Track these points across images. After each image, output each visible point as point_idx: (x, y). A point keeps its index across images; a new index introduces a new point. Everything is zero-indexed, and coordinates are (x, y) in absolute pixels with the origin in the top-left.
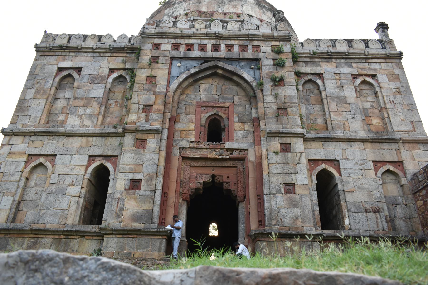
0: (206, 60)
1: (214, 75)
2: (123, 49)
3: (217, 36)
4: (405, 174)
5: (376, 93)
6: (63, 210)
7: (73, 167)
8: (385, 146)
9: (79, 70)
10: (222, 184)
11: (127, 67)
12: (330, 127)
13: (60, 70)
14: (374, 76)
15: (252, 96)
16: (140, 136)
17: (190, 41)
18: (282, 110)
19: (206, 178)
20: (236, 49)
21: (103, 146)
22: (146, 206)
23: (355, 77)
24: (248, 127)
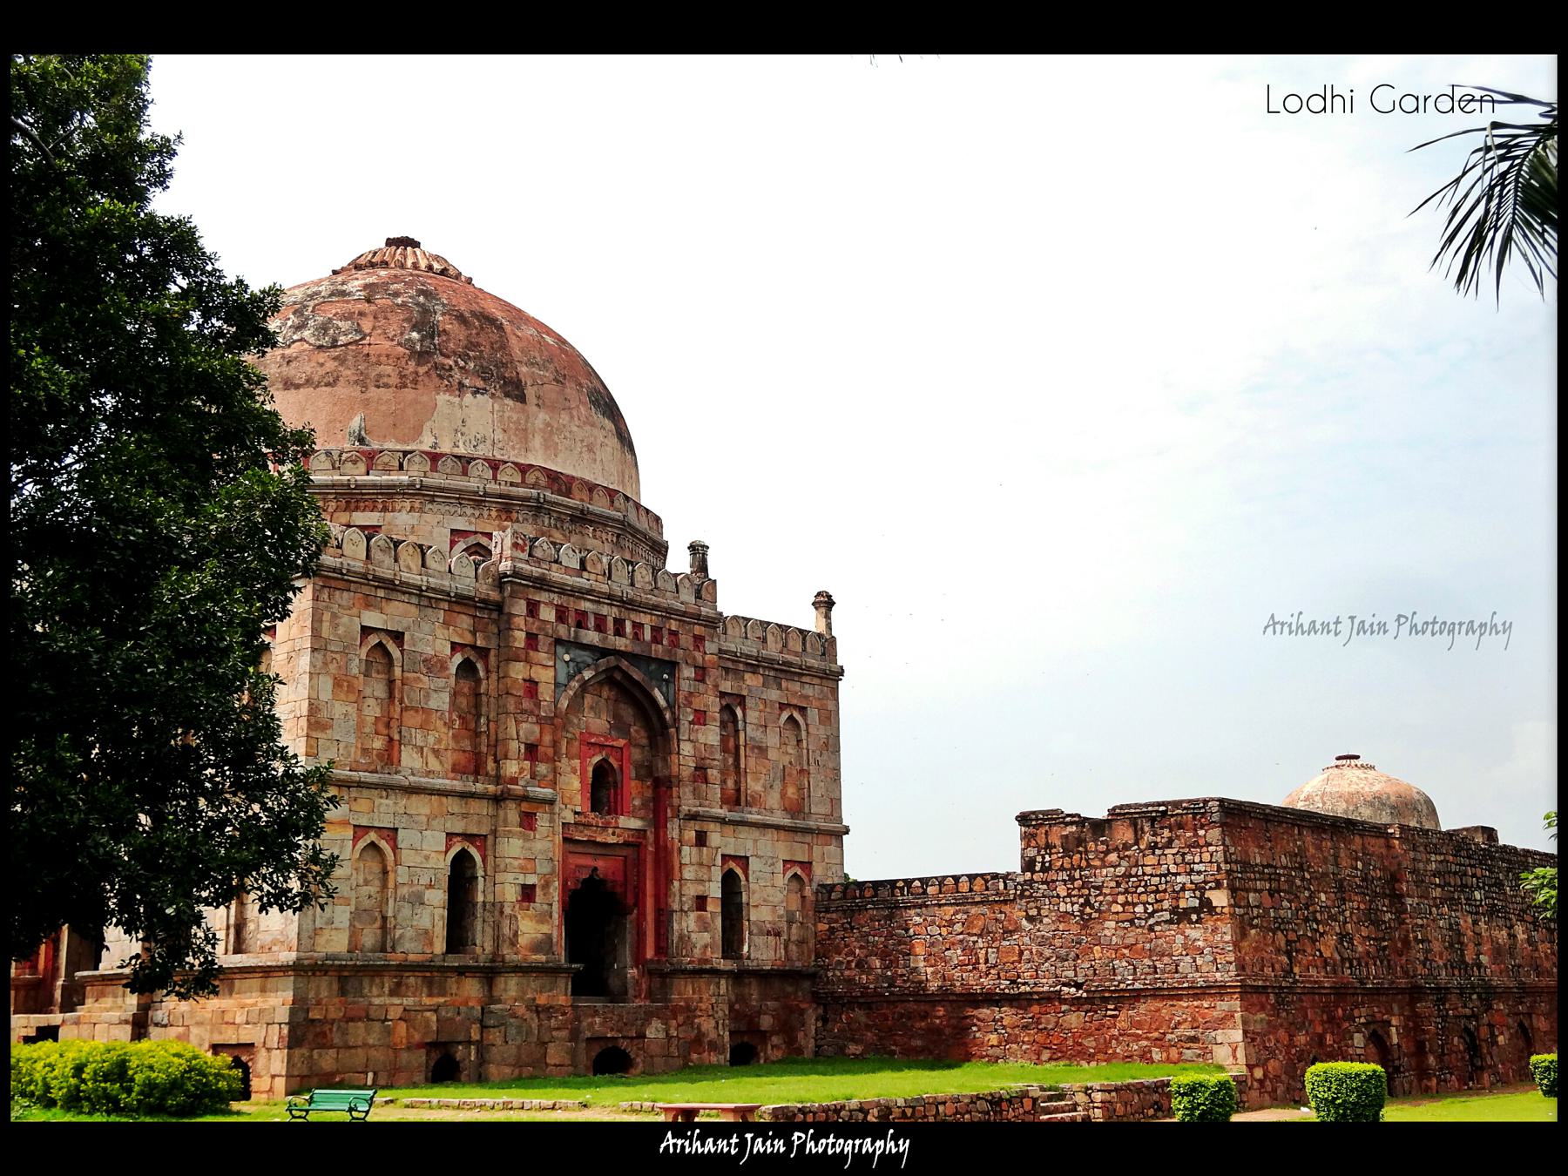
0: (603, 652)
2: (471, 599)
5: (799, 741)
6: (426, 932)
7: (426, 853)
9: (398, 637)
11: (479, 643)
13: (366, 631)
16: (525, 807)
18: (701, 773)
19: (585, 876)
21: (465, 816)
22: (545, 929)
23: (782, 706)
24: (649, 794)
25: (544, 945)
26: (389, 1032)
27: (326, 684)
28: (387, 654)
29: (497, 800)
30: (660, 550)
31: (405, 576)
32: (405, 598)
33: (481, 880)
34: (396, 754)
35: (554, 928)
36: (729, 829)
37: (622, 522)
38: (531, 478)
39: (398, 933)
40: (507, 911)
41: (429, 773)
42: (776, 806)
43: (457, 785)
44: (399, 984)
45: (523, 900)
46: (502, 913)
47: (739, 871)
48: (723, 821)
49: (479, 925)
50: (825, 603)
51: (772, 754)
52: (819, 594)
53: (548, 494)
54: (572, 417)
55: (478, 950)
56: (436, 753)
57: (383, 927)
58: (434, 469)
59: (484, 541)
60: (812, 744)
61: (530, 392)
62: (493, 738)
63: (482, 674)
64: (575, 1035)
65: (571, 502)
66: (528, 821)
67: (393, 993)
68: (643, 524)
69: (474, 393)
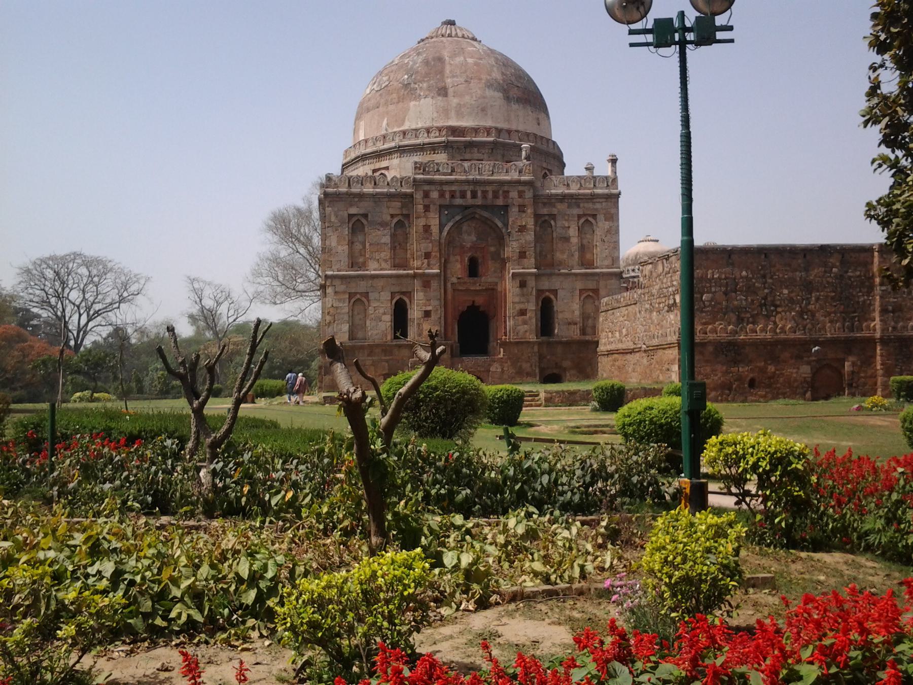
0: (467, 208)
1: (474, 218)
10: (478, 307)
19: (469, 304)
23: (579, 217)
47: (552, 297)
50: (614, 161)
56: (386, 261)
61: (451, 91)
67: (368, 355)
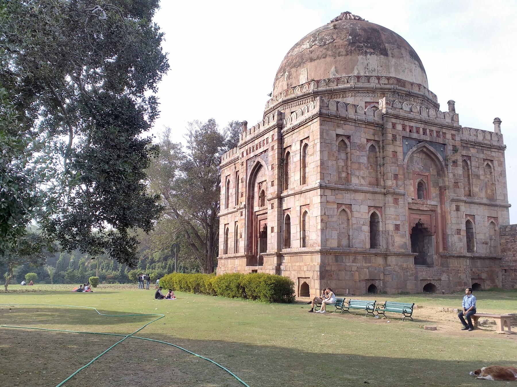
0: (420, 141)
2: (373, 123)
3: (426, 123)
4: (498, 224)
5: (491, 173)
7: (361, 213)
8: (493, 208)
9: (348, 137)
12: (472, 194)
13: (338, 135)
14: (492, 161)
15: (441, 172)
16: (395, 197)
17: (412, 124)
20: (435, 134)
23: (484, 160)
24: (438, 192)
25: (404, 245)
26: (352, 275)
27: (326, 153)
28: (345, 144)
29: (385, 194)
30: (437, 106)
31: (350, 116)
32: (350, 123)
33: (381, 222)
34: (350, 178)
35: (407, 240)
36: (467, 205)
37: (423, 96)
38: (391, 81)
39: (354, 241)
40: (390, 234)
41: (361, 185)
42: (484, 197)
43: (371, 189)
44: (355, 259)
45: (396, 230)
46: (388, 234)
48: (466, 202)
49: (381, 238)
50: (498, 122)
51: (482, 177)
52: (495, 119)
53: (397, 86)
54: (404, 60)
55: (381, 247)
56: (363, 178)
57: (349, 239)
58: (358, 81)
59: (376, 105)
60: (496, 174)
61: (389, 52)
62: (382, 173)
63: (377, 150)
64: (416, 278)
65: (405, 89)
66: (396, 201)
67: (354, 261)
68: (430, 97)
69: (370, 54)
